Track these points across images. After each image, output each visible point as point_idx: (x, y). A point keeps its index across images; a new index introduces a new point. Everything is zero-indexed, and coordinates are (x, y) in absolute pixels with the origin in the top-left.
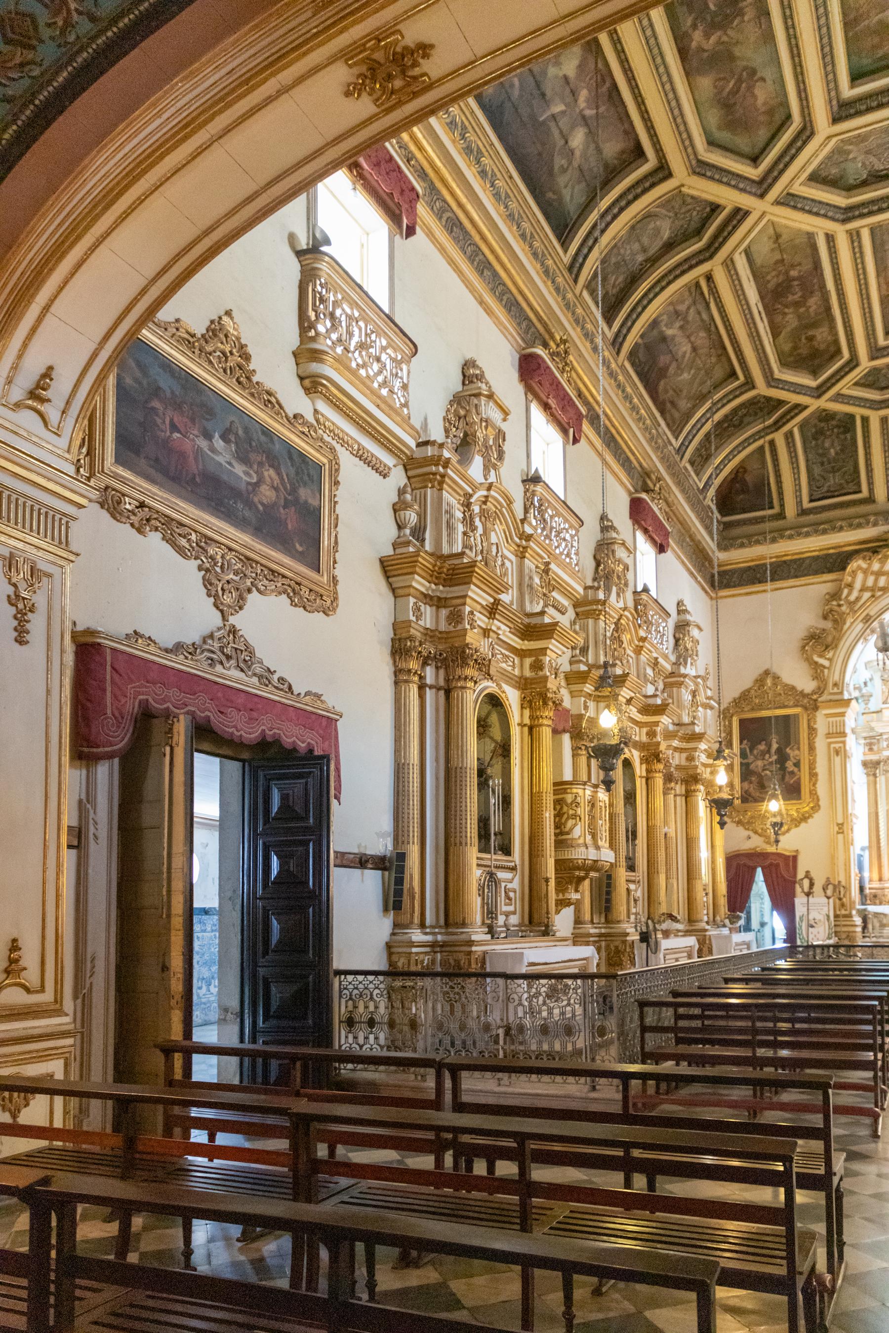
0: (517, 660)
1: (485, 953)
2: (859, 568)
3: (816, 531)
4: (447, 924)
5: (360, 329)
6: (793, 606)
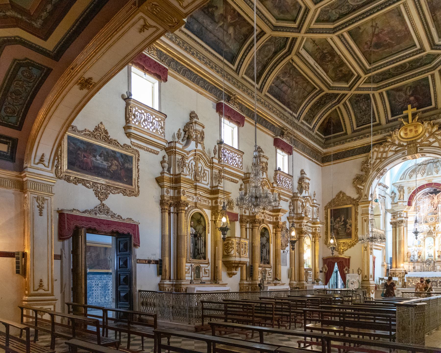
0: (210, 201)
2: (375, 151)
3: (358, 138)
4: (177, 279)
5: (145, 116)
6: (351, 167)
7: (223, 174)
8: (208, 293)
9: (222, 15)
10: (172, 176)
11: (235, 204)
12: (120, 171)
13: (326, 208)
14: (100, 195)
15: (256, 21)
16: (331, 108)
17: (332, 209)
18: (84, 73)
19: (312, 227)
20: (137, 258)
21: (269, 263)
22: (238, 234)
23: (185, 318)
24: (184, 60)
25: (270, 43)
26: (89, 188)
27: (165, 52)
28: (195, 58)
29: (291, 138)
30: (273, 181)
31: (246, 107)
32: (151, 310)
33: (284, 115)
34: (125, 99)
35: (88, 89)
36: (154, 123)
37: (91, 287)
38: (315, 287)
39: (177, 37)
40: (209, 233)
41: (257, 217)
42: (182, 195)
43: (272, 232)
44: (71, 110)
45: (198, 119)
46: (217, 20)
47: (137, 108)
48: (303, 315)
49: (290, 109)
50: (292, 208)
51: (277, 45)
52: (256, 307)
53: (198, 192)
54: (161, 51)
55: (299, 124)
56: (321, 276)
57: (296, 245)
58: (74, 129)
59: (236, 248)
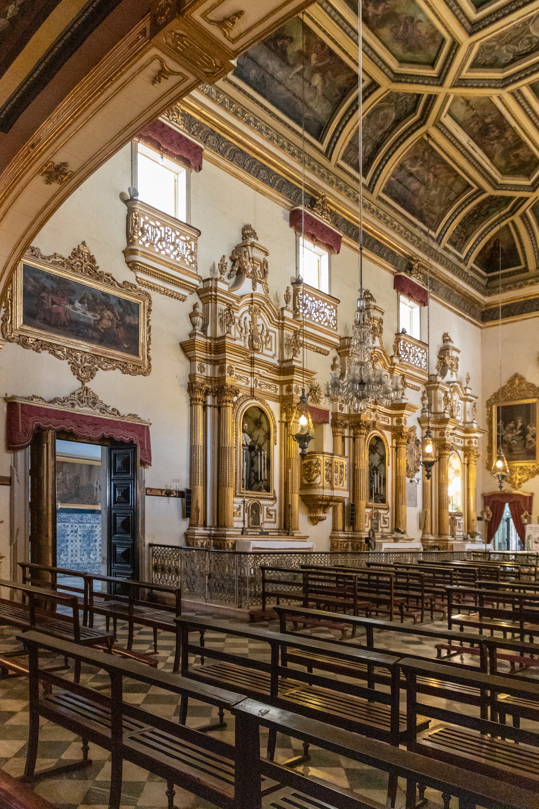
0: (278, 387)
1: (236, 541)
4: (218, 526)
5: (161, 231)
7: (301, 338)
8: (274, 553)
9: (300, 52)
10: (209, 341)
11: (322, 393)
12: (115, 328)
13: (489, 404)
14: (80, 372)
15: (361, 64)
16: (499, 223)
17: (501, 405)
18: (54, 154)
19: (463, 437)
20: (147, 485)
21: (384, 501)
22: (328, 447)
23: (232, 597)
24: (233, 132)
25: (387, 104)
26: (61, 359)
27: (198, 117)
28: (251, 128)
29: (425, 276)
30: (391, 353)
31: (344, 219)
32: (170, 581)
33: (412, 234)
34: (126, 202)
35: (61, 182)
36: (178, 245)
37: (63, 536)
38: (469, 546)
39: (219, 91)
40: (275, 444)
41: (363, 418)
42: (227, 374)
43: (390, 445)
44: (30, 220)
45: (257, 239)
46: (291, 62)
47: (147, 218)
48: (446, 596)
49: (424, 223)
50: (426, 402)
51: (401, 107)
52: (360, 579)
53: (256, 370)
54: (191, 116)
55: (440, 250)
56: (479, 527)
57: (434, 469)
58: (36, 254)
59: (325, 472)
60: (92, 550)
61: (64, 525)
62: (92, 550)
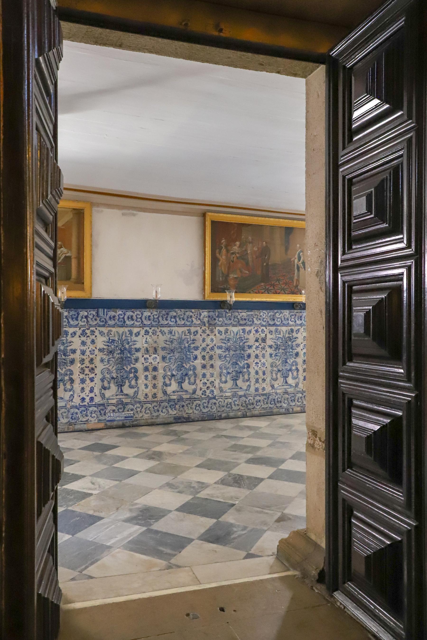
60: (290, 370)
61: (244, 331)
62: (290, 370)
